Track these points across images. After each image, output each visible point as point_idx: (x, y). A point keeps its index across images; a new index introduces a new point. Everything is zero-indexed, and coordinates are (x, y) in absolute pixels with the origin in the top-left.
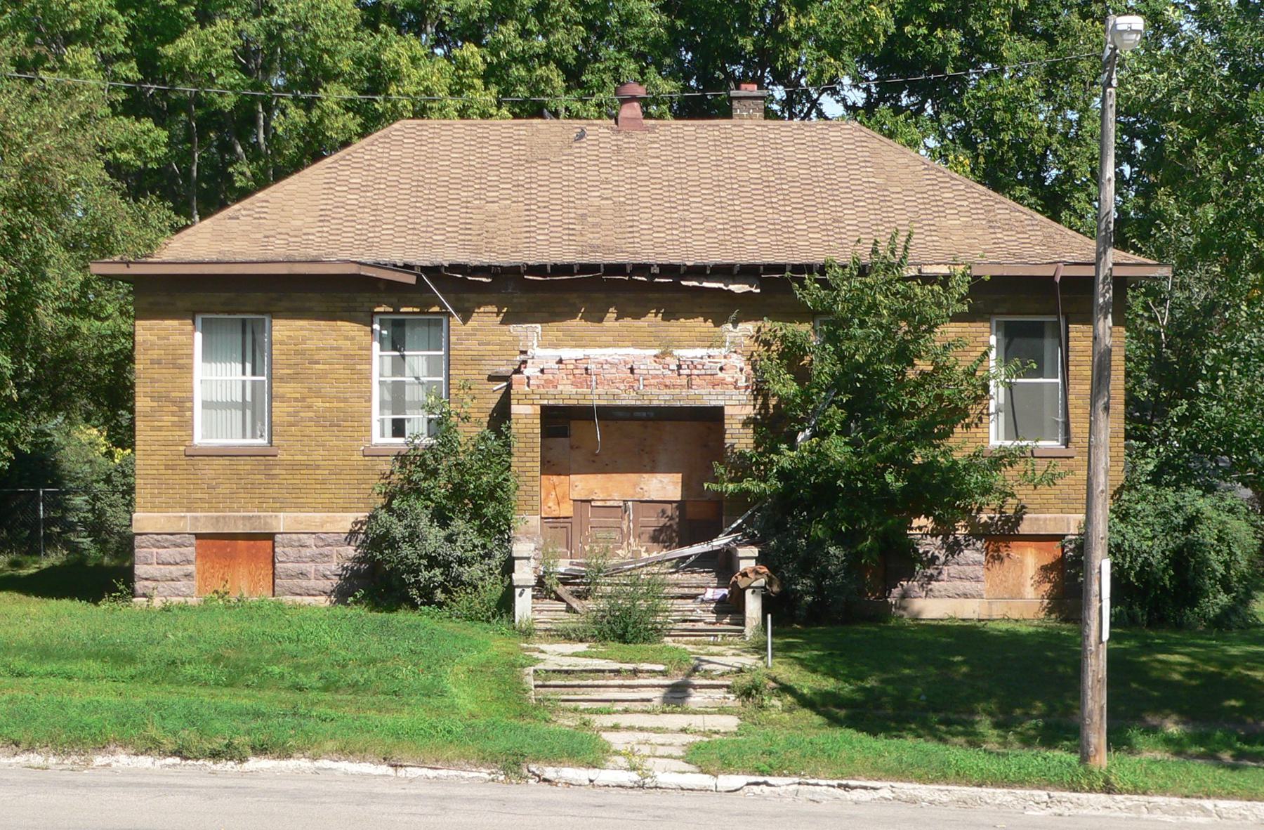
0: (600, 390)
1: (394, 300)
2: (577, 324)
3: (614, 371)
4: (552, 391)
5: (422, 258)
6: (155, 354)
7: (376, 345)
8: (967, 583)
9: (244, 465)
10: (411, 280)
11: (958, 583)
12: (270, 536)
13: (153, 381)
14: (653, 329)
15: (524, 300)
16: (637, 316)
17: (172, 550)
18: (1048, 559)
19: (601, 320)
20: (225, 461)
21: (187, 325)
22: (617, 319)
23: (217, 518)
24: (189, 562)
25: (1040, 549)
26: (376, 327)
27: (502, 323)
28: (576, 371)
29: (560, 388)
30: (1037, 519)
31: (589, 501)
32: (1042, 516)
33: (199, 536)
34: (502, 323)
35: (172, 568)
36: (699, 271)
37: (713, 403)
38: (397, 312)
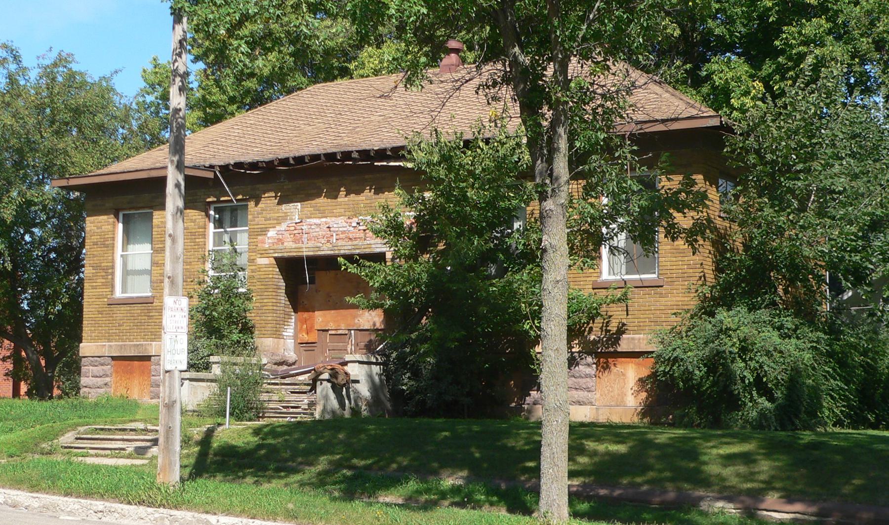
0: (310, 244)
1: (218, 193)
2: (322, 201)
3: (318, 230)
4: (280, 246)
5: (220, 160)
6: (95, 238)
7: (211, 225)
8: (581, 393)
9: (137, 309)
10: (210, 175)
11: (574, 392)
12: (148, 358)
13: (94, 256)
14: (368, 202)
15: (290, 186)
16: (358, 192)
17: (100, 368)
18: (645, 372)
19: (336, 197)
20: (127, 308)
21: (111, 218)
22: (346, 196)
23: (121, 346)
24: (107, 376)
25: (638, 364)
26: (212, 212)
27: (279, 204)
28: (296, 232)
29: (286, 244)
30: (633, 339)
31: (327, 331)
32: (637, 336)
33: (114, 358)
34: (279, 204)
35: (99, 379)
36: (381, 154)
37: (378, 250)
38: (219, 201)
